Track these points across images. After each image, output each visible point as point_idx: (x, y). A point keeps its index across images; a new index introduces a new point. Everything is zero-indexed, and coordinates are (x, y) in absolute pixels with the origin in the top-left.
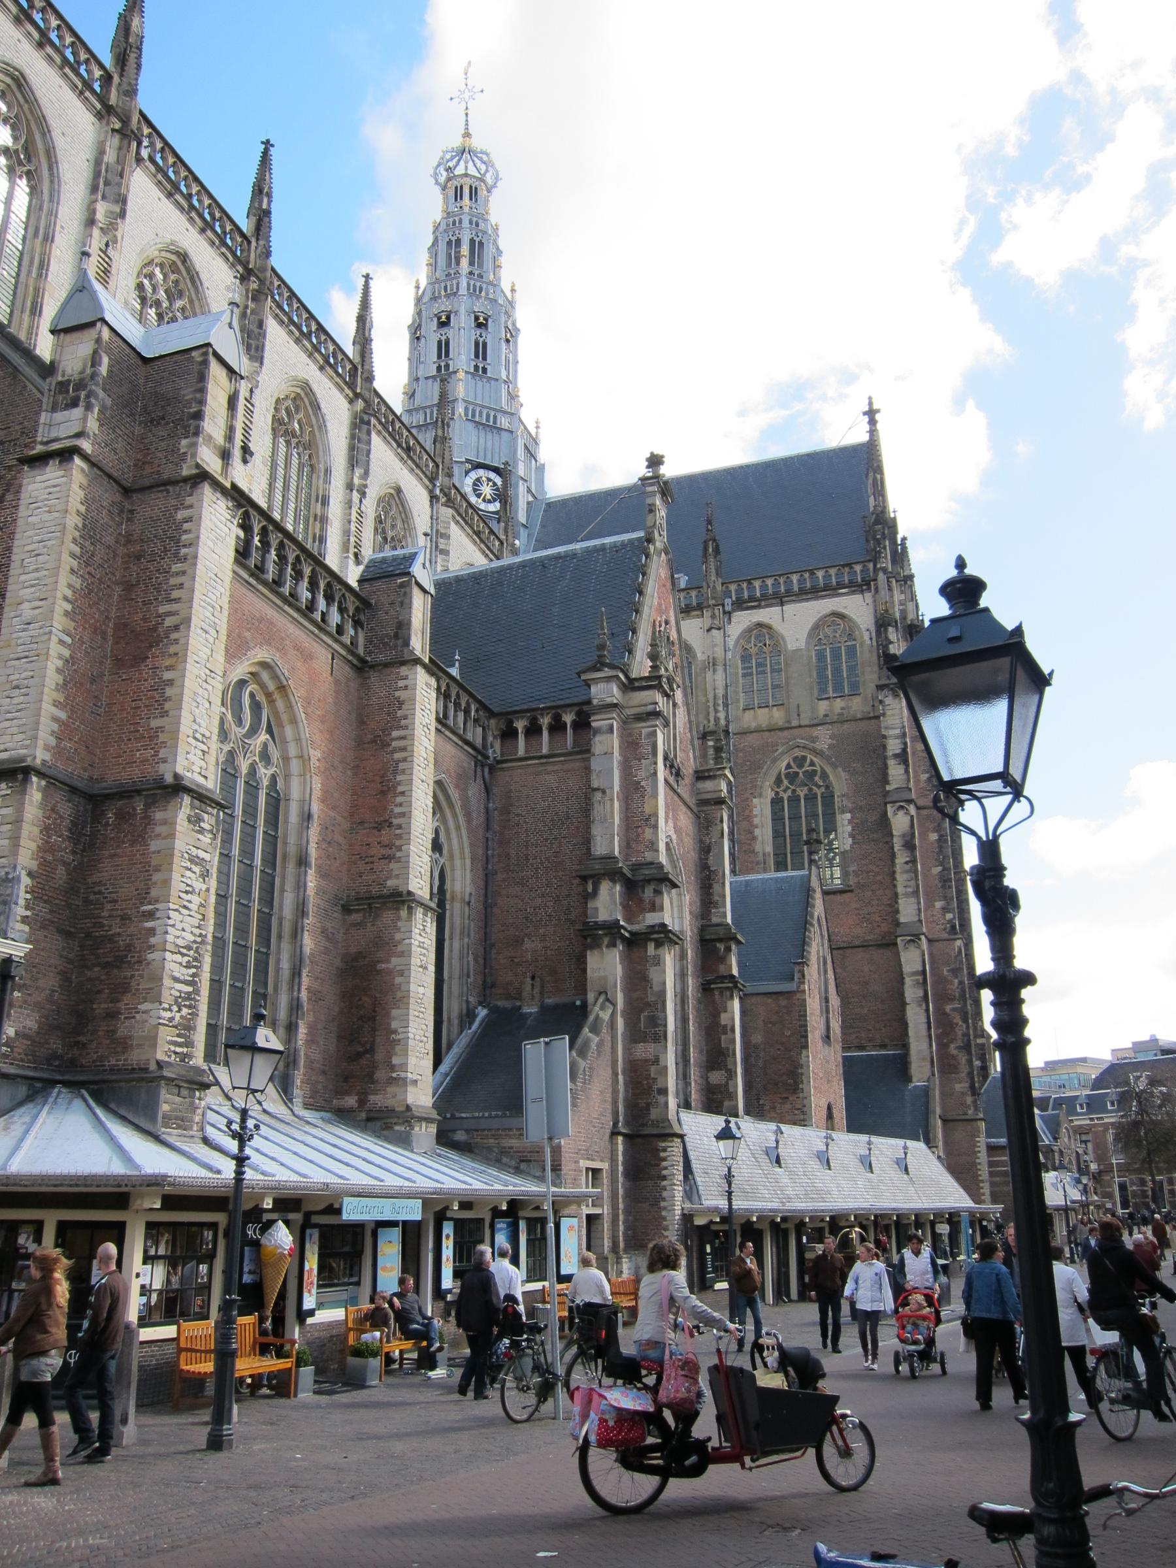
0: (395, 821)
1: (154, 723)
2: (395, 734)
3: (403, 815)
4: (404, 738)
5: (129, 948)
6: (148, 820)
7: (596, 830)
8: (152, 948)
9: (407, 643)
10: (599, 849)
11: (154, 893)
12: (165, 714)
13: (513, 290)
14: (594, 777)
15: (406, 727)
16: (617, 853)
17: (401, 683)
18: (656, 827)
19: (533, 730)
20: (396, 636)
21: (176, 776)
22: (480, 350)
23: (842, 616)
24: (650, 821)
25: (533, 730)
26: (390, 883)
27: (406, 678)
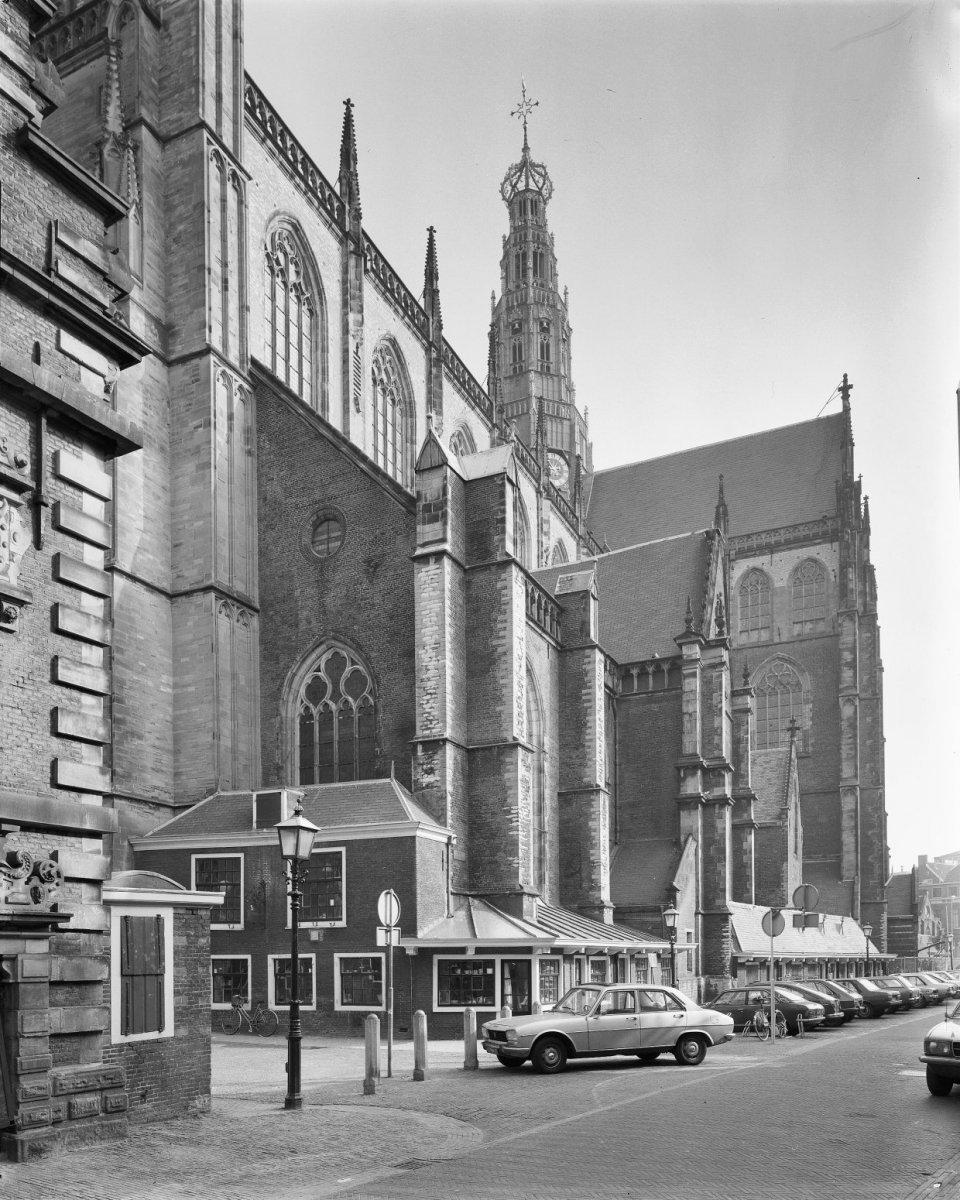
0: (587, 744)
1: (498, 709)
2: (584, 691)
3: (591, 740)
4: (590, 694)
5: (499, 829)
6: (503, 762)
7: (686, 739)
8: (511, 829)
9: (588, 635)
10: (688, 749)
11: (509, 800)
12: (503, 704)
13: (566, 293)
14: (684, 704)
15: (590, 688)
16: (698, 752)
17: (586, 660)
18: (721, 735)
19: (643, 674)
20: (581, 630)
21: (515, 739)
22: (545, 350)
23: (815, 561)
24: (718, 732)
25: (643, 674)
26: (585, 780)
27: (589, 657)
